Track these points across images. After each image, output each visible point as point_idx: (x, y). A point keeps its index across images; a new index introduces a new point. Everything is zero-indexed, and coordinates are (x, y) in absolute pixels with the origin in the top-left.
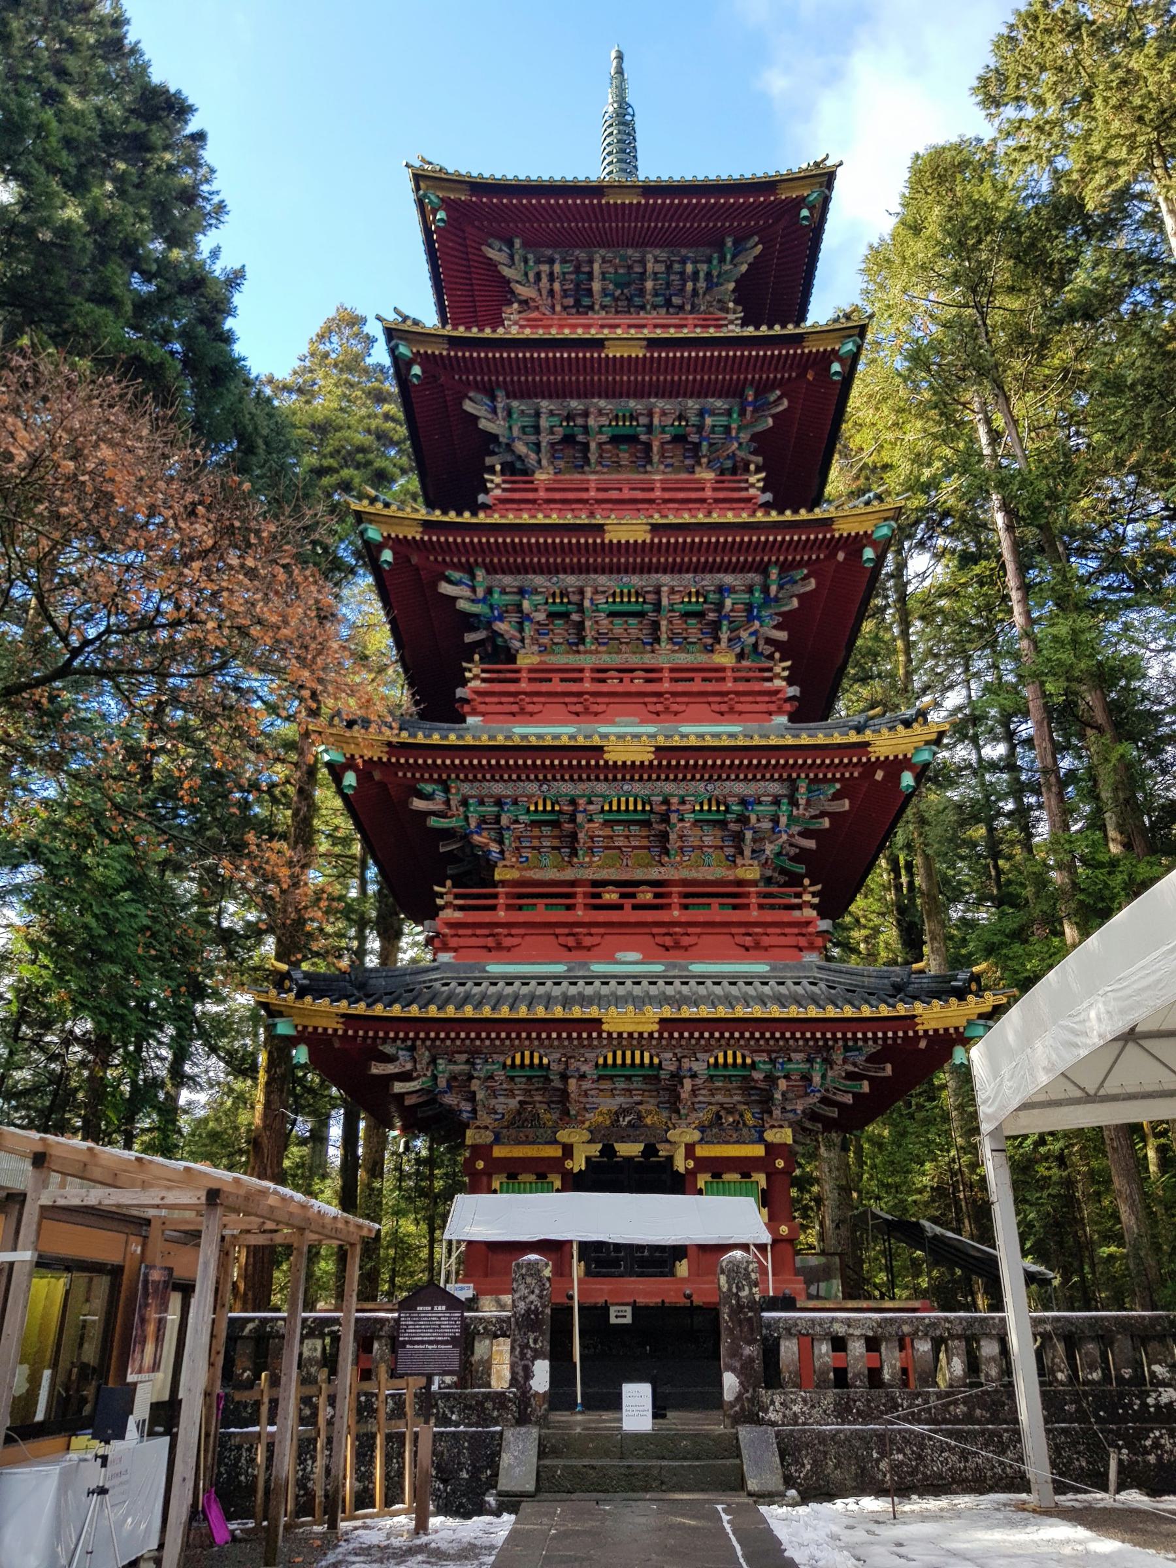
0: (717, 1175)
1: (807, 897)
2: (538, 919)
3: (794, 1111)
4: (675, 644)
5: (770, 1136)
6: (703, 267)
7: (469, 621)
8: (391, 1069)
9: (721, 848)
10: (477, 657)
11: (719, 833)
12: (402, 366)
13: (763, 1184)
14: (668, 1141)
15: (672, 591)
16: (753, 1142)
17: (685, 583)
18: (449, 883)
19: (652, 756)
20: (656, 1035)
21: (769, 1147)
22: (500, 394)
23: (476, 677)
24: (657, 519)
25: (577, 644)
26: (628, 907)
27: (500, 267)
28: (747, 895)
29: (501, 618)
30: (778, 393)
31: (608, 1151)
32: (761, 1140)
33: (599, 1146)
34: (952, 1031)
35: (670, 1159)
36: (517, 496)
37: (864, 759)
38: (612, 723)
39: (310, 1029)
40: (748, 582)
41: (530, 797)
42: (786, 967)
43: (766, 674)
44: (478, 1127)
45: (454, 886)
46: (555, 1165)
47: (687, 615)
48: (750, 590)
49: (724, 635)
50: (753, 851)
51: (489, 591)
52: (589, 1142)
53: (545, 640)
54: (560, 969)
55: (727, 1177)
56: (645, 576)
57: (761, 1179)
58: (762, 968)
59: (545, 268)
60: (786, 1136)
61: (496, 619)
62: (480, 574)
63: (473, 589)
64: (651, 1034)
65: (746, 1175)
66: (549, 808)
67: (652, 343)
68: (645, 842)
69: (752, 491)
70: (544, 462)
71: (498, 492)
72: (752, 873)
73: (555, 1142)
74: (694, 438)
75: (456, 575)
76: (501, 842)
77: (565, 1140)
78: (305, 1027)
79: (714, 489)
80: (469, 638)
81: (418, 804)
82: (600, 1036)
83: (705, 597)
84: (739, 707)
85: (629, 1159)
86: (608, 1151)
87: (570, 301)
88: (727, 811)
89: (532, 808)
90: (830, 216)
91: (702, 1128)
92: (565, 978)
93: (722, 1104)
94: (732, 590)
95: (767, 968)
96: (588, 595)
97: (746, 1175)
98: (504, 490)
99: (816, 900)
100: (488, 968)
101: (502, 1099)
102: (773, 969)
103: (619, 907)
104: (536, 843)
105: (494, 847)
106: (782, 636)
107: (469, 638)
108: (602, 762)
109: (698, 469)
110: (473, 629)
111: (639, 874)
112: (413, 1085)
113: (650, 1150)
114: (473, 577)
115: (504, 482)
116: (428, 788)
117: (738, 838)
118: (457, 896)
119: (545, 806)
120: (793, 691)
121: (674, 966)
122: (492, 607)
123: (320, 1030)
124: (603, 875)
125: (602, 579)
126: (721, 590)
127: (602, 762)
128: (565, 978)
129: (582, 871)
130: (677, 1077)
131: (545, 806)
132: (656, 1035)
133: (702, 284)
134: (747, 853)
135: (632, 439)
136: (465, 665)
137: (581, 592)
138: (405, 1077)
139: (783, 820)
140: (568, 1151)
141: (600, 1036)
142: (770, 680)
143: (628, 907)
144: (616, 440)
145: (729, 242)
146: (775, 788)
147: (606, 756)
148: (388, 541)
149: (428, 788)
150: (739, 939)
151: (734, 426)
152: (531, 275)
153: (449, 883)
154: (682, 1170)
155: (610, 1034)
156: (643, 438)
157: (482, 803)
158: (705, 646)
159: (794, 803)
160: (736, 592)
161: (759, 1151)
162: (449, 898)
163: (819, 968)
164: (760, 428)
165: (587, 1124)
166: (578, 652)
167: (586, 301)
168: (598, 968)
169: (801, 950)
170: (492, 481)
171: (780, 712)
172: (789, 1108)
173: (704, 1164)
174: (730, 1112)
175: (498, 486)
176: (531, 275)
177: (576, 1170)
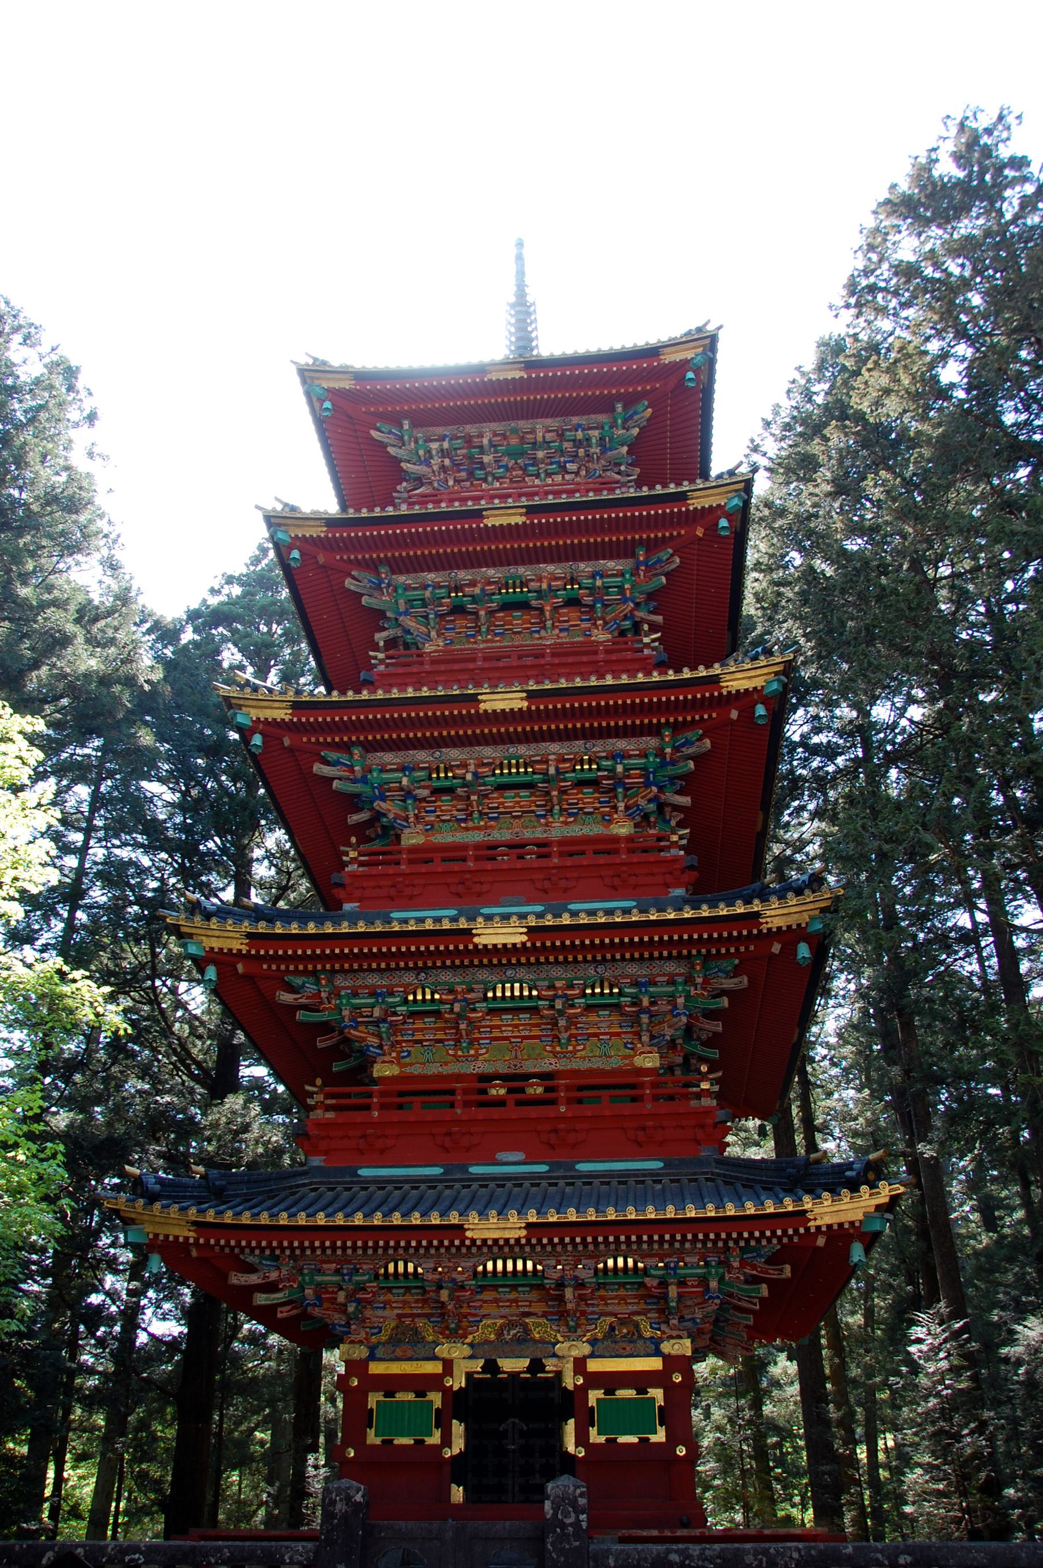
1: (705, 1085)
2: (412, 1119)
3: (693, 1319)
4: (570, 815)
5: (666, 1347)
6: (595, 434)
7: (354, 802)
8: (254, 1279)
9: (618, 1034)
10: (353, 840)
11: (615, 1018)
12: (283, 550)
14: (555, 1355)
17: (575, 750)
18: (319, 1081)
19: (524, 938)
20: (523, 1241)
21: (667, 1359)
22: (383, 569)
23: (353, 860)
24: (532, 686)
25: (465, 821)
26: (511, 1103)
27: (390, 449)
28: (641, 1086)
30: (670, 551)
31: (490, 1366)
32: (658, 1353)
33: (481, 1362)
34: (846, 1226)
35: (559, 1374)
37: (755, 932)
38: (497, 904)
39: (161, 1238)
40: (642, 746)
41: (406, 986)
44: (352, 1342)
45: (324, 1084)
46: (434, 1382)
47: (581, 784)
48: (644, 755)
49: (621, 806)
50: (652, 1037)
52: (471, 1357)
53: (431, 818)
54: (437, 1171)
56: (533, 745)
57: (657, 1394)
59: (434, 446)
60: (684, 1347)
61: (376, 798)
64: (518, 1240)
66: (428, 997)
67: (531, 511)
68: (536, 1032)
70: (433, 634)
71: (382, 668)
73: (435, 1358)
75: (332, 756)
76: (379, 1036)
77: (445, 1355)
78: (156, 1235)
80: (354, 818)
81: (286, 997)
82: (462, 1242)
85: (514, 1375)
86: (490, 1366)
87: (463, 474)
88: (621, 994)
89: (411, 997)
90: (717, 377)
91: (593, 1342)
92: (440, 1181)
94: (625, 755)
95: (661, 1164)
96: (472, 768)
98: (387, 665)
99: (716, 1088)
100: (360, 1172)
101: (380, 1313)
104: (419, 1036)
105: (373, 1041)
106: (685, 800)
107: (354, 818)
108: (471, 947)
110: (358, 810)
111: (529, 1067)
112: (278, 1297)
113: (536, 1366)
115: (388, 657)
116: (298, 981)
117: (636, 1020)
118: (328, 1096)
119: (424, 994)
120: (693, 860)
122: (374, 788)
123: (171, 1238)
124: (488, 1068)
125: (488, 752)
126: (613, 756)
127: (471, 947)
128: (440, 1181)
129: (466, 1065)
130: (560, 1285)
131: (424, 994)
132: (523, 1241)
133: (595, 450)
134: (645, 1038)
135: (524, 606)
136: (342, 848)
137: (464, 765)
138: (270, 1287)
140: (448, 1366)
141: (462, 1242)
142: (669, 847)
143: (511, 1103)
144: (507, 607)
145: (619, 407)
146: (671, 967)
147: (476, 940)
149: (298, 981)
152: (421, 452)
153: (319, 1081)
154: (570, 1387)
155: (473, 1241)
156: (534, 603)
157: (355, 995)
158: (603, 815)
159: (689, 980)
160: (630, 757)
161: (654, 1364)
162: (320, 1097)
165: (468, 1340)
166: (467, 829)
167: (479, 473)
168: (474, 1170)
170: (375, 658)
172: (687, 1317)
174: (623, 1322)
175: (382, 662)
176: (421, 452)
177: (456, 1388)
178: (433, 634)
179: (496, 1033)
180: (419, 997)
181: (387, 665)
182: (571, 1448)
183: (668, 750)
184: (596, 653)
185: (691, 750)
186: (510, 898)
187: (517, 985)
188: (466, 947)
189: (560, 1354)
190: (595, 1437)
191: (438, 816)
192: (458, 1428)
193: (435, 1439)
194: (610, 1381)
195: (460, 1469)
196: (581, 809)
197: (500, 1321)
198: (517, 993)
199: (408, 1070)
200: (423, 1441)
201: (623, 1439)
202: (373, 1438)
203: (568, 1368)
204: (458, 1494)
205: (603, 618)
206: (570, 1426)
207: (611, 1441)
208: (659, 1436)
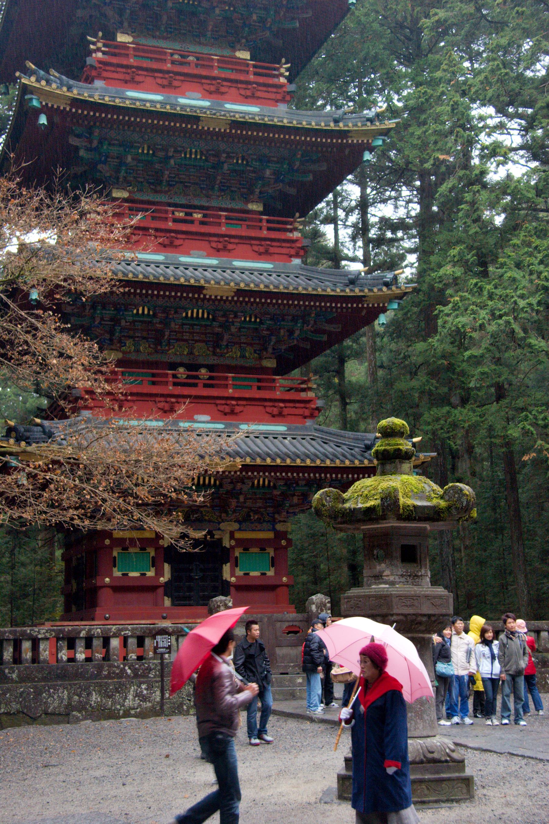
0: (246, 549)
5: (279, 527)
13: (272, 554)
14: (219, 529)
15: (229, 157)
16: (269, 530)
29: (105, 163)
32: (274, 529)
35: (220, 540)
36: (115, 60)
42: (296, 428)
43: (289, 227)
51: (100, 142)
55: (252, 550)
58: (282, 428)
61: (101, 162)
62: (97, 132)
63: (91, 142)
65: (263, 549)
69: (282, 80)
70: (126, 24)
72: (270, 363)
74: (239, 22)
75: (78, 130)
79: (255, 74)
83: (247, 162)
84: (272, 250)
88: (261, 323)
93: (250, 508)
97: (263, 549)
102: (289, 429)
103: (195, 385)
104: (131, 333)
109: (238, 46)
111: (201, 361)
114: (91, 133)
121: (231, 425)
122: (100, 154)
127: (202, 296)
134: (270, 350)
139: (297, 333)
142: (291, 231)
147: (205, 292)
148: (45, 109)
150: (268, 409)
151: (269, 20)
154: (228, 546)
157: (104, 308)
161: (270, 535)
163: (316, 430)
164: (288, 25)
169: (305, 417)
171: (297, 256)
173: (241, 543)
174: (256, 512)
177: (166, 546)
178: (126, 24)
179: (179, 336)
180: (140, 312)
181: (104, 53)
182: (228, 580)
183: (298, 163)
184: (247, 72)
185: (312, 167)
186: (196, 252)
187: (200, 311)
188: (199, 296)
189: (222, 528)
190: (239, 572)
191: (134, 178)
192: (167, 567)
193: (151, 573)
194: (246, 545)
195: (169, 589)
196: (228, 187)
197: (186, 509)
198: (200, 315)
199: (128, 356)
200: (127, 574)
201: (252, 574)
202: (117, 573)
203: (228, 536)
204: (167, 602)
205: (246, 38)
206: (226, 569)
207: (247, 574)
208: (271, 573)
